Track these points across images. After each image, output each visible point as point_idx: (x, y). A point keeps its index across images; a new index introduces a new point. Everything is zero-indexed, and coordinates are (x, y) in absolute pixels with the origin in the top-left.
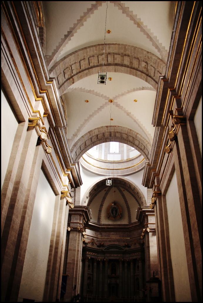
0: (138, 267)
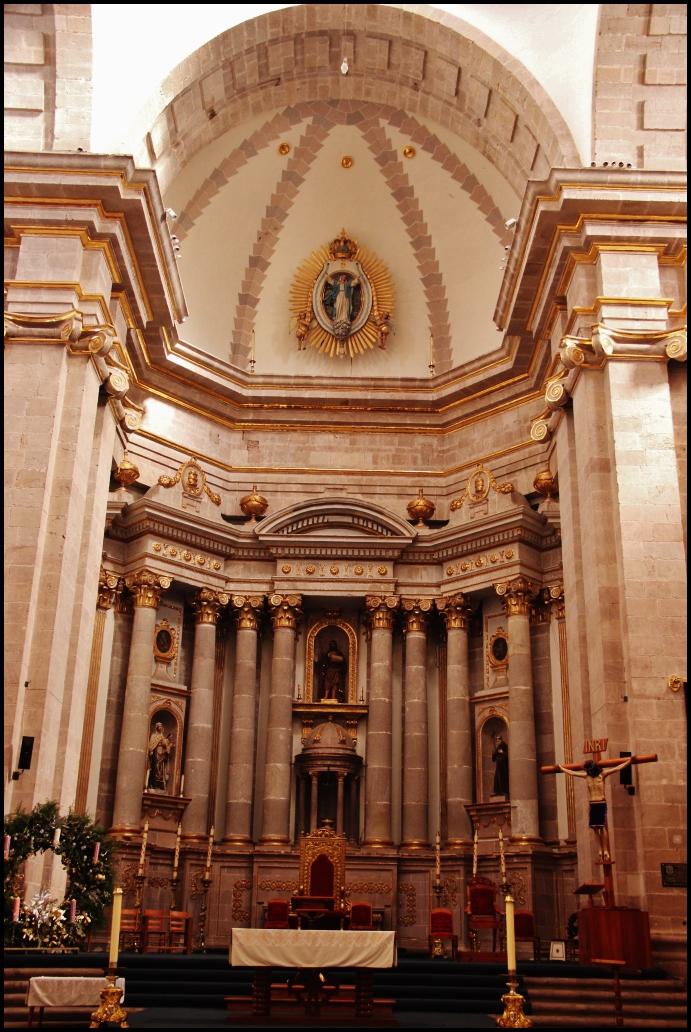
0: (500, 648)
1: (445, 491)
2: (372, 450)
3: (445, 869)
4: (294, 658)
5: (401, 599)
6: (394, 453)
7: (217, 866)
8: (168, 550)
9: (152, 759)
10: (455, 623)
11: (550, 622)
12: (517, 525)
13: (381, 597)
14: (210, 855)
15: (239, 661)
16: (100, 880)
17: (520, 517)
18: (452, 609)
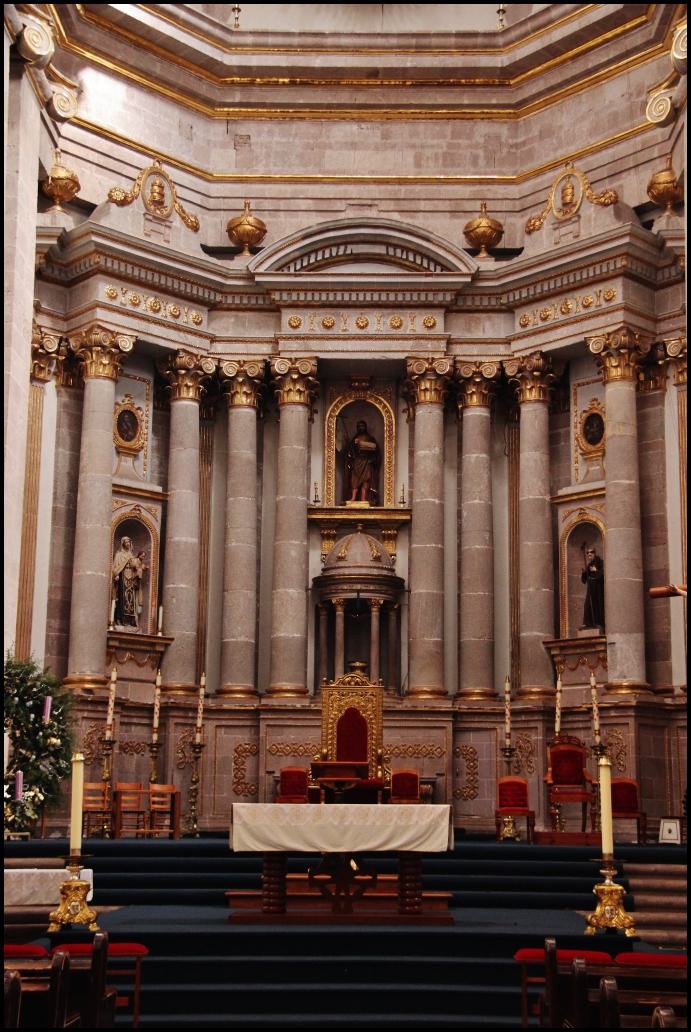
0: (594, 428)
1: (518, 206)
2: (413, 146)
3: (518, 725)
4: (309, 446)
5: (455, 362)
6: (445, 149)
7: (211, 725)
8: (127, 296)
9: (118, 584)
10: (531, 394)
11: (666, 390)
12: (624, 250)
14: (200, 711)
15: (233, 451)
16: (54, 745)
17: (626, 240)
18: (527, 374)
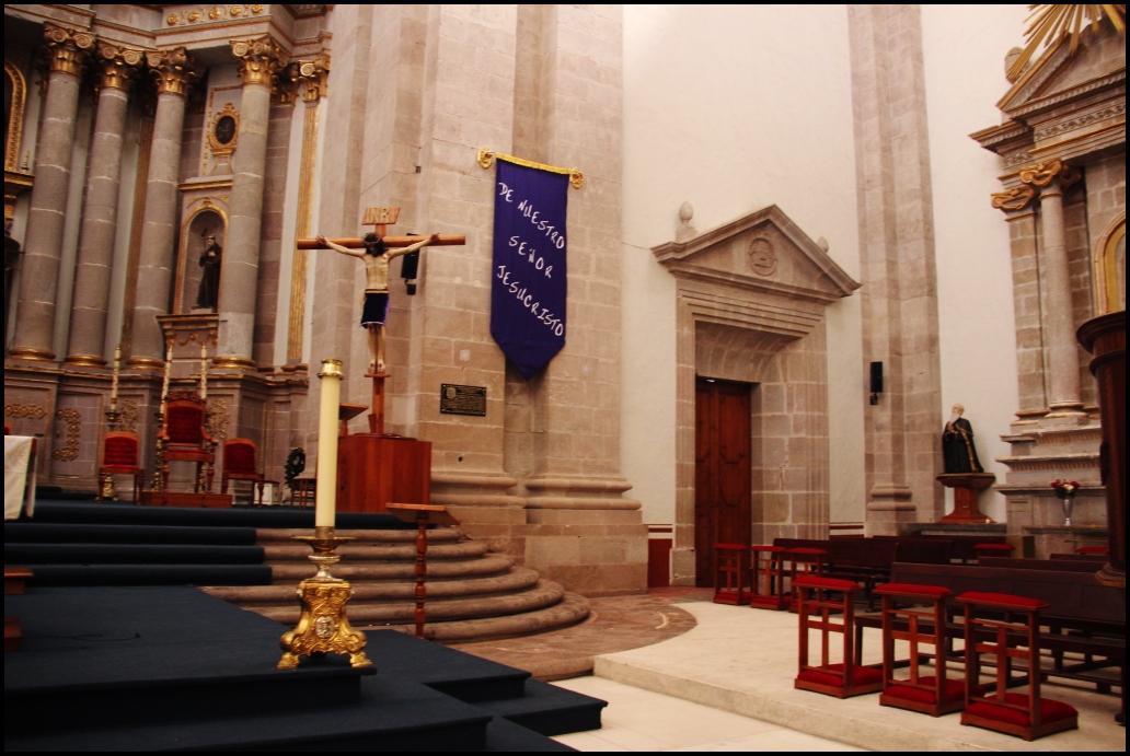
0: (226, 129)
3: (124, 393)
13: (68, 31)
18: (169, 68)
